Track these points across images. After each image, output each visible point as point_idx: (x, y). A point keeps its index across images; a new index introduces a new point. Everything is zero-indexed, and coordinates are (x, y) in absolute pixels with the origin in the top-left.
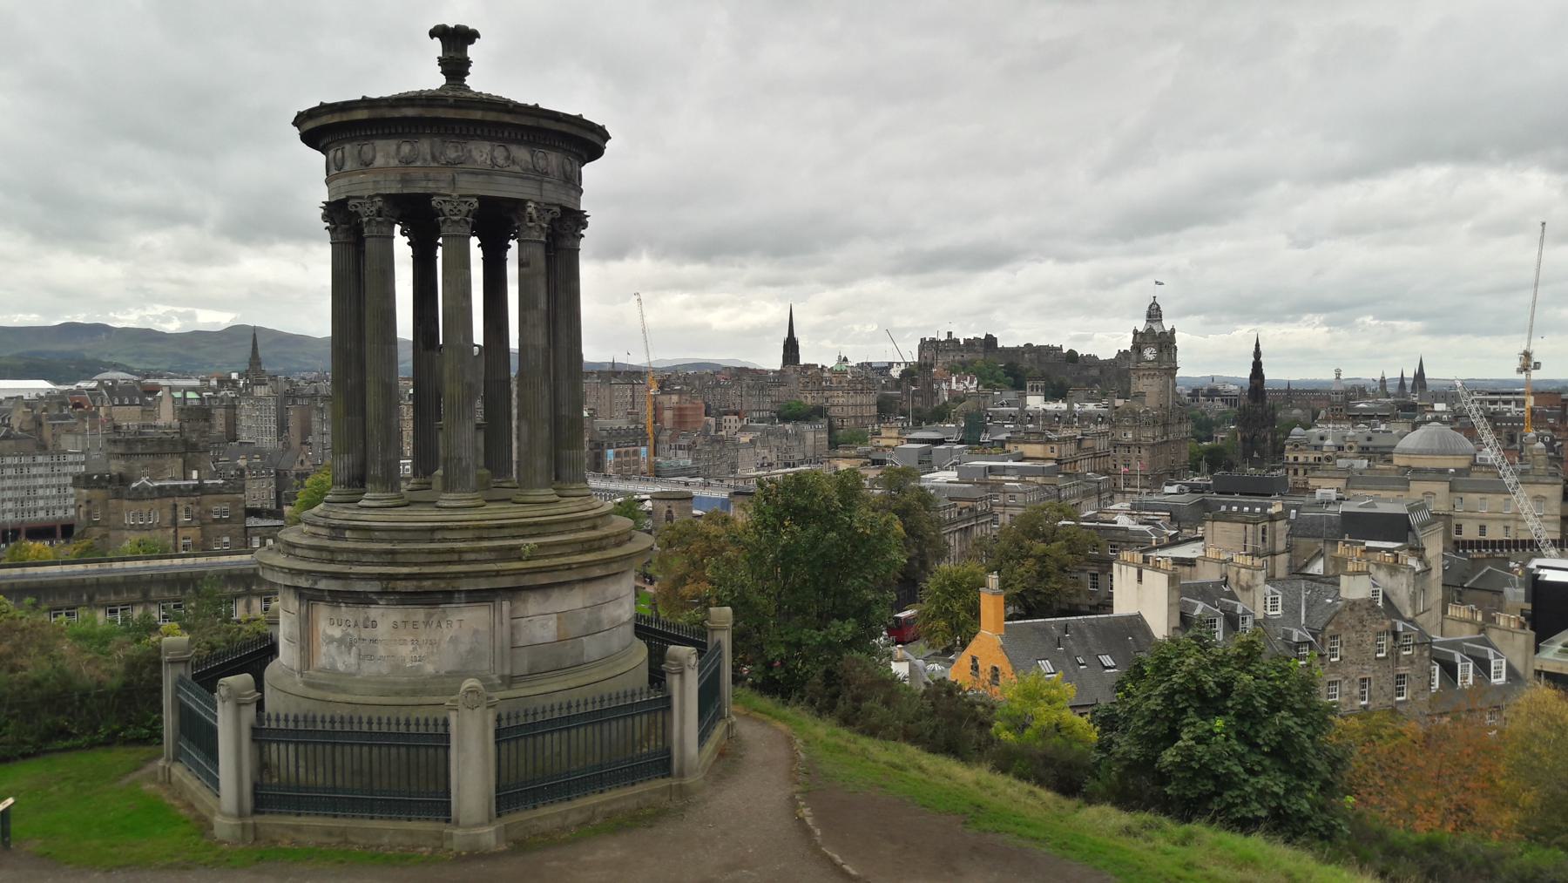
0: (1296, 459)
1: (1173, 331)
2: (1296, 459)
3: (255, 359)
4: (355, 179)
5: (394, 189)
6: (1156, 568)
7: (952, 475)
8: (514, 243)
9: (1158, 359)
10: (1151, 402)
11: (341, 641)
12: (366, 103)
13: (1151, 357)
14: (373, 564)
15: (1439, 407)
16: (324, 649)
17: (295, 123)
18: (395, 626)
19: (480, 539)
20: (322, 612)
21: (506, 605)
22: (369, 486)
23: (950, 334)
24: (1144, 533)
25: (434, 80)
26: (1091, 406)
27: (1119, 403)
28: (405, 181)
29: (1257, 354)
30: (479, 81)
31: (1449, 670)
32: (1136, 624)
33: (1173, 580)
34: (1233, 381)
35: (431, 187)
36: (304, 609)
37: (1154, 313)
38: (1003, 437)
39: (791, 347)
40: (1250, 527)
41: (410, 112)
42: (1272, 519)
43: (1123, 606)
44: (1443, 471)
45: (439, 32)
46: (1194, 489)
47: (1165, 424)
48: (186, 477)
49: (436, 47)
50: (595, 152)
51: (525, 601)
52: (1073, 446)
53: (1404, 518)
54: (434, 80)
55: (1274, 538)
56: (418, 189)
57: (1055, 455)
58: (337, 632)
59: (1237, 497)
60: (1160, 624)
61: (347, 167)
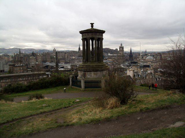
3: (20, 52)
5: (91, 37)
6: (131, 70)
15: (149, 54)
26: (115, 55)
30: (94, 27)
31: (156, 79)
32: (129, 76)
33: (133, 71)
35: (94, 37)
37: (121, 45)
41: (93, 31)
43: (128, 74)
44: (150, 61)
46: (129, 63)
50: (104, 33)
53: (149, 66)
54: (90, 27)
58: (88, 74)
60: (132, 76)
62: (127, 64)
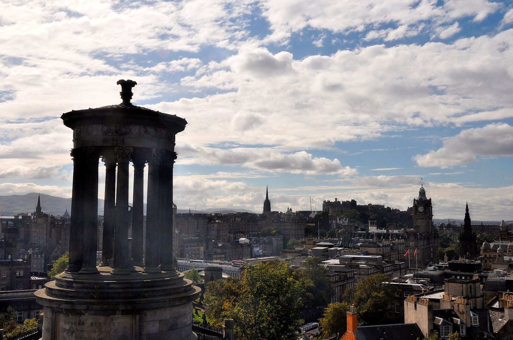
0: (486, 256)
1: (430, 199)
2: (486, 256)
7: (337, 261)
8: (147, 165)
9: (425, 212)
10: (422, 230)
11: (69, 331)
12: (90, 110)
14: (84, 298)
16: (61, 334)
17: (62, 117)
18: (92, 324)
19: (128, 288)
20: (62, 318)
21: (138, 317)
22: (83, 265)
23: (336, 199)
24: (419, 287)
25: (117, 101)
26: (396, 231)
29: (467, 210)
32: (414, 328)
33: (430, 308)
34: (459, 221)
36: (54, 316)
37: (422, 193)
38: (359, 244)
39: (267, 204)
40: (464, 285)
42: (474, 282)
45: (121, 82)
46: (440, 268)
47: (428, 239)
48: (6, 258)
49: (120, 88)
51: (146, 315)
52: (389, 248)
54: (117, 101)
55: (475, 290)
57: (381, 253)
58: (67, 327)
59: (459, 272)
60: (424, 327)
62: (430, 270)
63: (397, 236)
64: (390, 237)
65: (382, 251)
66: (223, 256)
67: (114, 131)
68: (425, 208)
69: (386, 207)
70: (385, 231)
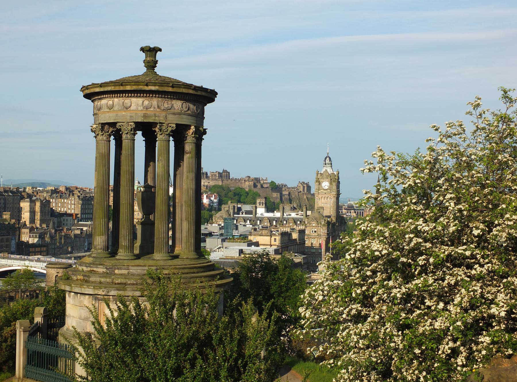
4: (120, 114)
9: (330, 188)
13: (326, 188)
26: (293, 215)
27: (309, 213)
28: (145, 116)
30: (161, 70)
35: (157, 120)
49: (143, 55)
52: (286, 238)
56: (151, 120)
61: (116, 108)
63: (295, 221)
64: (285, 222)
65: (277, 240)
66: (45, 249)
67: (156, 107)
68: (331, 184)
69: (269, 181)
70: (278, 214)
